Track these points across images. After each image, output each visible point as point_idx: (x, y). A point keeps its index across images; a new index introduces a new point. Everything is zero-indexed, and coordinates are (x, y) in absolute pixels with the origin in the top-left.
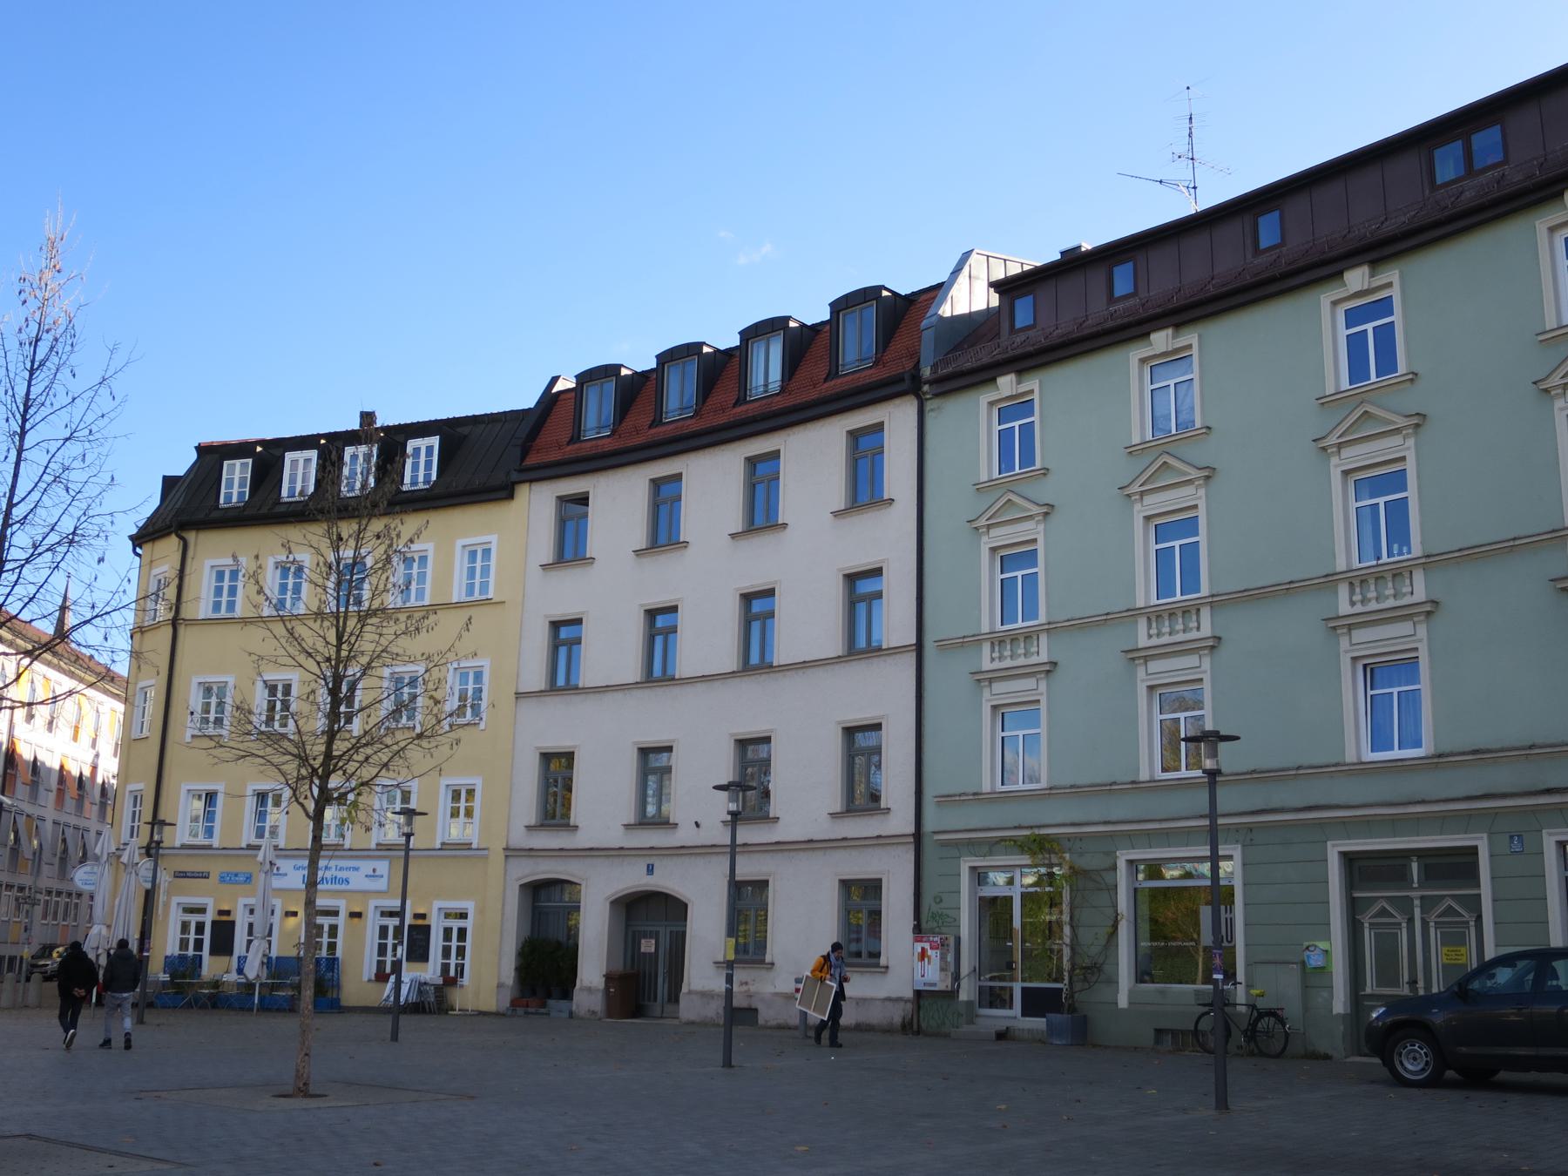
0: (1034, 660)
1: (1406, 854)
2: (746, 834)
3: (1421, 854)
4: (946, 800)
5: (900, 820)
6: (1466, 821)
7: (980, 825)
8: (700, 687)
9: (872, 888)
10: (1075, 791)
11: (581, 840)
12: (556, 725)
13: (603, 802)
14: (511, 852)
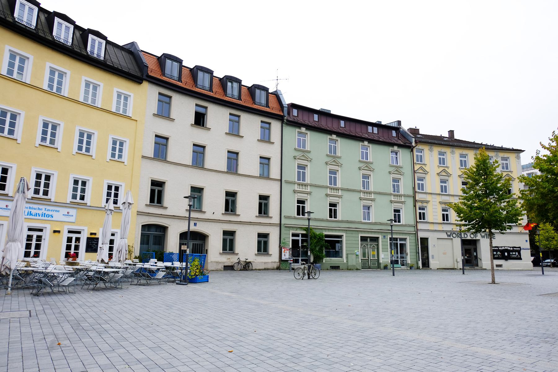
0: (306, 190)
4: (286, 217)
5: (275, 219)
8: (214, 173)
9: (266, 236)
12: (159, 172)
14: (140, 213)
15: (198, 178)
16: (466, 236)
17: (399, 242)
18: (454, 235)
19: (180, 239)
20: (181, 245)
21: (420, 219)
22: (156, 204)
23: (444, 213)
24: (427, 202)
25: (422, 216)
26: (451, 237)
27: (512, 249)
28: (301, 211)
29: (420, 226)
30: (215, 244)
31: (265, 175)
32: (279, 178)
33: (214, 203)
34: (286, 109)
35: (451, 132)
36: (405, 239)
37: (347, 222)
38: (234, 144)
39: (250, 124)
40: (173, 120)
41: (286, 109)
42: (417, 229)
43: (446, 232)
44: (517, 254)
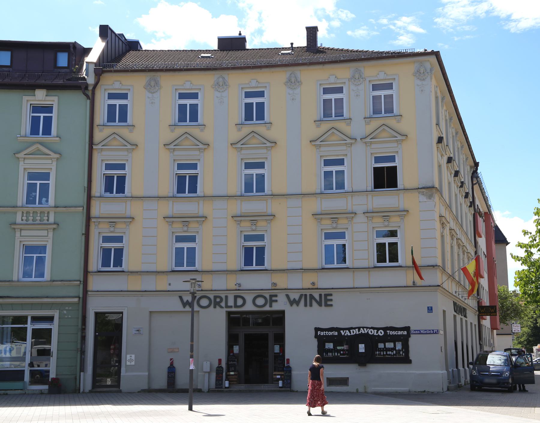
16: (240, 302)
27: (381, 333)
42: (85, 291)
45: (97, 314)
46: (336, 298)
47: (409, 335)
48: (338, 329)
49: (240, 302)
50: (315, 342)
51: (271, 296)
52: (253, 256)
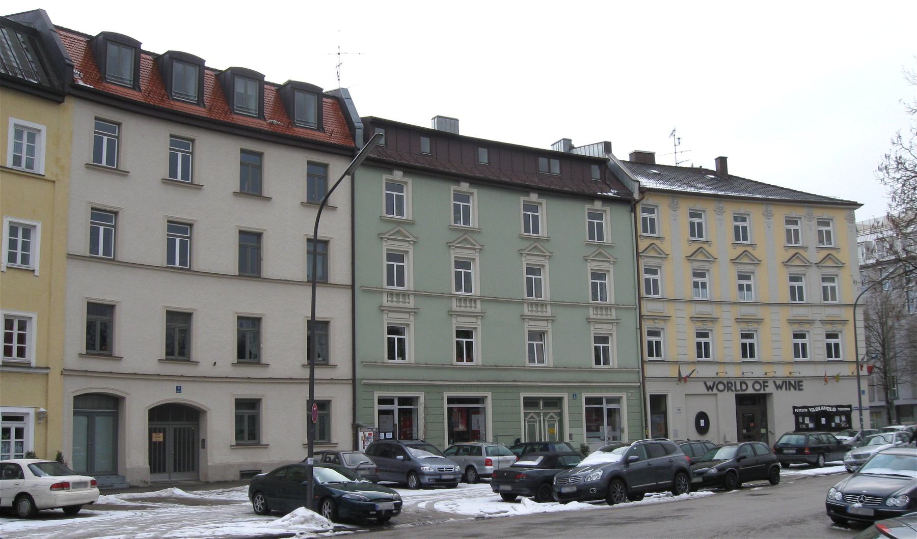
0: (407, 305)
1: (539, 398)
2: (319, 373)
3: (543, 398)
5: (343, 370)
6: (561, 388)
7: (384, 377)
10: (428, 367)
11: (124, 367)
12: (101, 284)
13: (139, 340)
14: (67, 373)
15: (181, 294)
16: (744, 387)
17: (605, 406)
18: (721, 387)
19: (150, 420)
20: (151, 431)
21: (651, 355)
22: (98, 351)
23: (700, 340)
24: (666, 318)
25: (654, 349)
26: (715, 391)
27: (834, 410)
28: (396, 349)
29: (651, 371)
30: (219, 427)
31: (317, 276)
32: (349, 282)
33: (214, 343)
34: (359, 133)
35: (722, 162)
36: (617, 400)
37: (497, 368)
38: (251, 215)
39: (285, 170)
40: (125, 173)
41: (359, 133)
42: (644, 377)
43: (704, 380)
44: (843, 418)
45: (651, 396)
46: (805, 384)
47: (851, 411)
48: (807, 407)
49: (744, 387)
50: (793, 417)
51: (764, 382)
52: (748, 351)
